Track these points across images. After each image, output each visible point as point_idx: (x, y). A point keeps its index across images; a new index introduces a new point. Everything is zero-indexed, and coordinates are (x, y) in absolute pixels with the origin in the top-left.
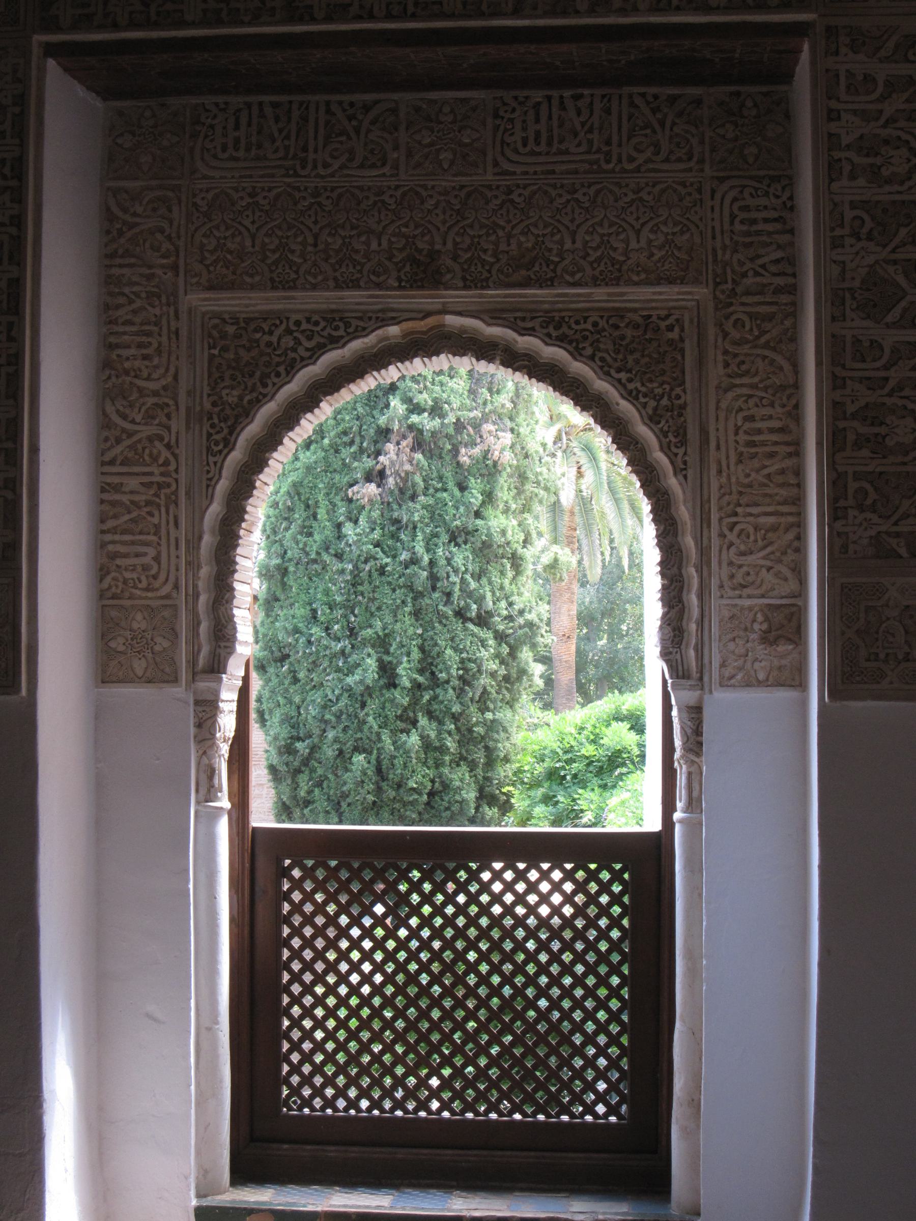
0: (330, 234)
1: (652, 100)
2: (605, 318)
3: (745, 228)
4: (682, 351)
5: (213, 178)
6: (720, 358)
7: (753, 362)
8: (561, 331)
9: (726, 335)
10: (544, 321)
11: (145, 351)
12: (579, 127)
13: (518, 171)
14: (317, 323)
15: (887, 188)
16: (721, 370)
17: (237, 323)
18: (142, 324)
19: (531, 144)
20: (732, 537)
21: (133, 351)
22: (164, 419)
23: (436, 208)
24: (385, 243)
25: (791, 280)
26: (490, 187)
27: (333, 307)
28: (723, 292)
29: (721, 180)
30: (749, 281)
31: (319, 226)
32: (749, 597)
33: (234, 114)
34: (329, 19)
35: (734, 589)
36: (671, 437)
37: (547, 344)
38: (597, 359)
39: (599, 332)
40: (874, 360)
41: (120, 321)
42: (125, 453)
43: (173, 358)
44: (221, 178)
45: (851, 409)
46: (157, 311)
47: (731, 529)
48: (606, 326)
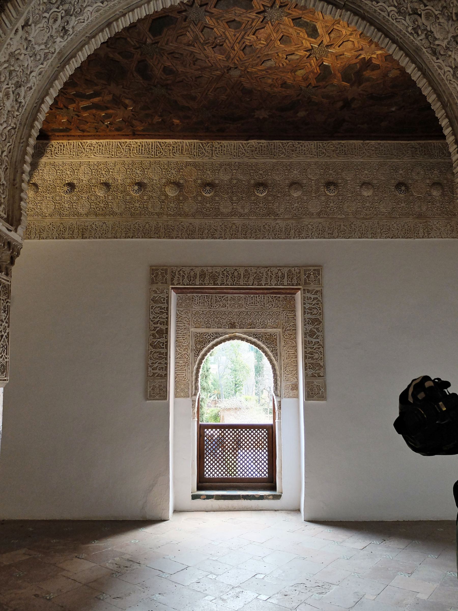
4: (277, 340)
15: (313, 316)
20: (285, 372)
29: (283, 311)
34: (221, 285)
46: (186, 331)
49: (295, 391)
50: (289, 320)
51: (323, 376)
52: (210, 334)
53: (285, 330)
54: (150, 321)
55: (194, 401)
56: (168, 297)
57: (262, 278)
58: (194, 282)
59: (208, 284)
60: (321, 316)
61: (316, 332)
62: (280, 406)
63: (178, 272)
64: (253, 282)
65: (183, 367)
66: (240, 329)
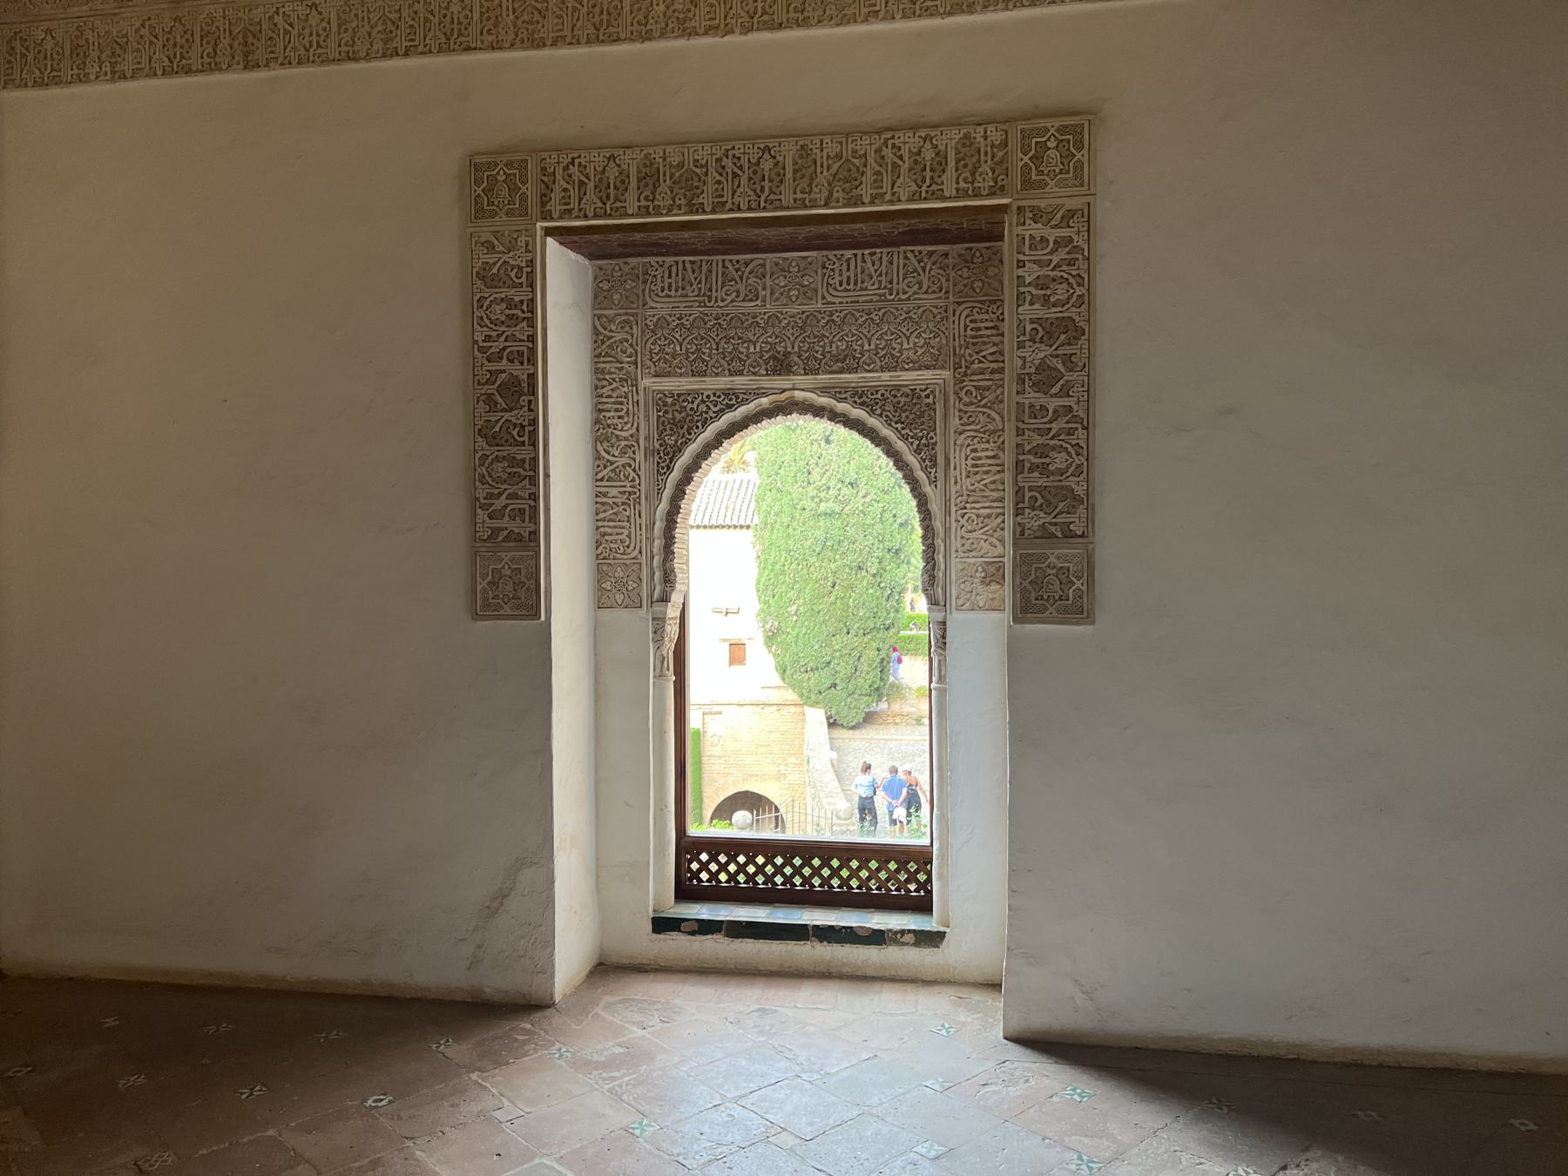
0: (725, 343)
3: (973, 333)
4: (935, 410)
5: (656, 308)
6: (957, 414)
9: (960, 400)
11: (620, 414)
12: (873, 273)
13: (837, 302)
15: (1054, 310)
16: (957, 421)
17: (673, 397)
18: (617, 397)
20: (963, 521)
21: (612, 414)
22: (632, 455)
24: (758, 349)
26: (820, 312)
27: (729, 387)
29: (959, 304)
30: (976, 366)
32: (974, 557)
34: (713, 212)
39: (885, 400)
43: (636, 418)
44: (662, 308)
45: (1027, 448)
46: (626, 389)
47: (963, 517)
49: (994, 587)
51: (1082, 536)
52: (708, 397)
53: (965, 374)
54: (476, 353)
55: (659, 622)
56: (531, 263)
57: (863, 173)
58: (618, 204)
61: (1063, 370)
62: (944, 637)
64: (831, 195)
65: (621, 509)
66: (806, 374)
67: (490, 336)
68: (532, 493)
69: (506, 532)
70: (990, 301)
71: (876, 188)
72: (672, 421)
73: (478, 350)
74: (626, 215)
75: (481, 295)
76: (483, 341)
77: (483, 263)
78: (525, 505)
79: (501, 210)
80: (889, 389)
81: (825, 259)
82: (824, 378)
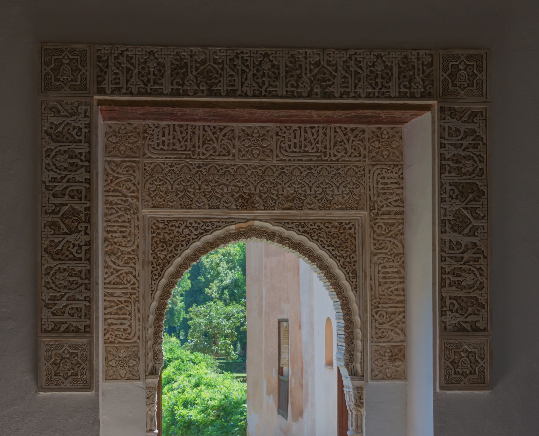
0: (206, 185)
1: (344, 130)
2: (323, 224)
3: (383, 186)
5: (153, 158)
6: (372, 241)
7: (386, 243)
8: (304, 229)
10: (297, 224)
12: (313, 141)
13: (287, 159)
14: (199, 224)
15: (464, 177)
17: (164, 223)
19: (293, 149)
21: (118, 234)
22: (133, 265)
23: (252, 175)
25: (402, 209)
26: (274, 166)
27: (207, 216)
28: (373, 213)
29: (373, 165)
30: (384, 209)
31: (201, 181)
32: (384, 342)
33: (162, 129)
34: (227, 96)
35: (377, 338)
36: (350, 274)
37: (298, 234)
38: (319, 241)
39: (320, 229)
40: (458, 249)
41: (112, 220)
42: (115, 279)
44: (157, 158)
46: (129, 217)
48: (323, 227)
50: (388, 189)
51: (485, 330)
53: (378, 214)
56: (89, 126)
59: (195, 94)
60: (484, 176)
62: (360, 398)
63: (115, 58)
66: (265, 209)
67: (55, 178)
68: (88, 296)
69: (66, 326)
70: (394, 165)
71: (344, 87)
72: (163, 241)
73: (45, 188)
74: (162, 94)
75: (49, 147)
76: (50, 181)
77: (51, 123)
78: (81, 305)
79: (65, 85)
80: (323, 222)
81: (278, 130)
82: (277, 213)
